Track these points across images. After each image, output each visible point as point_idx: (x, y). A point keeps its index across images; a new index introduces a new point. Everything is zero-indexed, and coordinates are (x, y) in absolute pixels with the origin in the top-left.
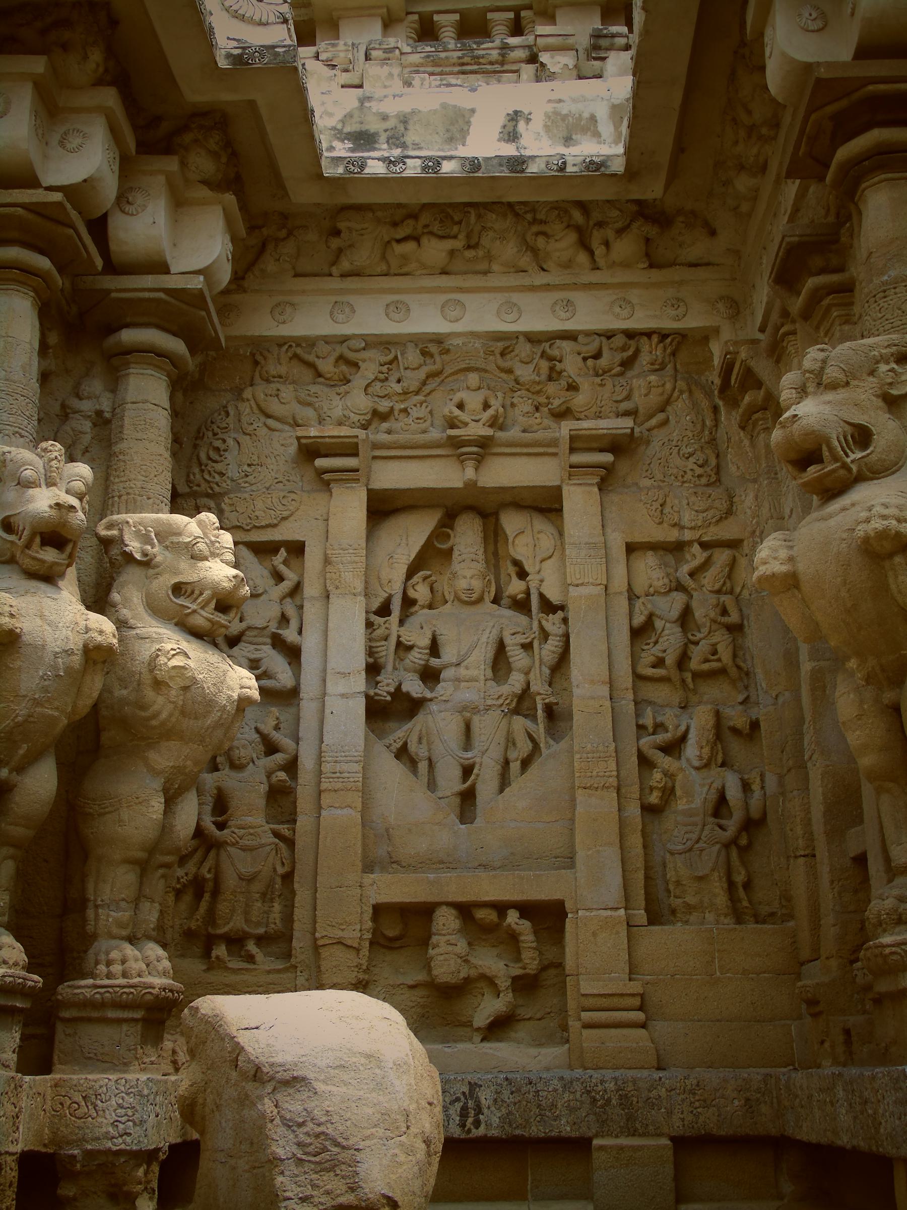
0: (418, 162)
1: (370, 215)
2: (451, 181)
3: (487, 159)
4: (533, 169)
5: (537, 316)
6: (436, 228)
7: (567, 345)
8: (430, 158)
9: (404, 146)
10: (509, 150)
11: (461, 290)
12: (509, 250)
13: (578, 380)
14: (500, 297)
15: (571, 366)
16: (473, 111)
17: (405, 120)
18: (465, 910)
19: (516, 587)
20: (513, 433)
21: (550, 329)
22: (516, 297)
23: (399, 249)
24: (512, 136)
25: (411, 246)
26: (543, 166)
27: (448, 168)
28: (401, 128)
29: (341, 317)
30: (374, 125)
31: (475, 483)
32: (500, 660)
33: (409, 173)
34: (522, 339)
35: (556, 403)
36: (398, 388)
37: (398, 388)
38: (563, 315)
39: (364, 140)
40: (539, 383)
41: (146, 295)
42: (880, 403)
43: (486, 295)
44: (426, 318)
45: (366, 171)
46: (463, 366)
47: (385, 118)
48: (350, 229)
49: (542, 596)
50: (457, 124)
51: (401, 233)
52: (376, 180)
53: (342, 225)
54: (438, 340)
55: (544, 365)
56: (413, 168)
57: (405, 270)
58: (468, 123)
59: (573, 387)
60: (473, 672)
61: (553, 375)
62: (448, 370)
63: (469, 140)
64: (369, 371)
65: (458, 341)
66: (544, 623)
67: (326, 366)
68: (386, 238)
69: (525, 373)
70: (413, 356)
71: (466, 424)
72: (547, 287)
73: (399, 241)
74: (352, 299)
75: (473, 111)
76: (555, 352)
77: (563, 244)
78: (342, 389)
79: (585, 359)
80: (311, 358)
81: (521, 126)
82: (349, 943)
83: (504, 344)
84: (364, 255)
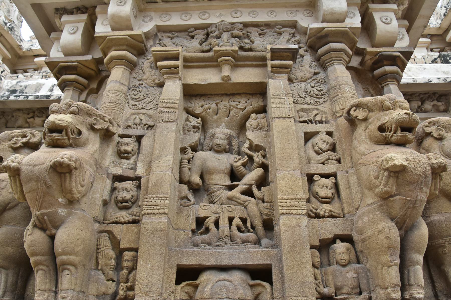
0: (23, 97)
1: (22, 111)
3: (41, 96)
6: (38, 115)
8: (26, 96)
9: (23, 93)
10: (49, 93)
16: (44, 84)
17: (26, 87)
25: (32, 120)
28: (24, 88)
30: (18, 88)
33: (20, 99)
39: (13, 92)
42: (10, 149)
45: (9, 99)
47: (21, 86)
48: (16, 115)
50: (39, 87)
51: (29, 116)
52: (11, 101)
53: (14, 114)
56: (21, 98)
58: (41, 87)
63: (40, 91)
73: (29, 118)
75: (44, 84)
84: (20, 122)
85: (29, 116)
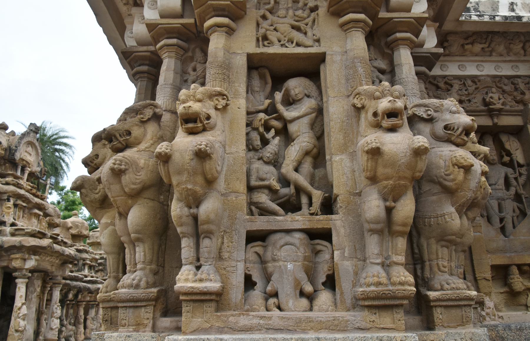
0: (488, 17)
2: (498, 23)
4: (524, 20)
5: (506, 70)
7: (519, 80)
11: (482, 61)
12: (501, 48)
13: (524, 91)
14: (494, 64)
15: (522, 86)
18: (519, 267)
19: (506, 159)
20: (508, 107)
21: (513, 74)
22: (499, 64)
23: (466, 47)
24: (513, 10)
26: (527, 19)
27: (497, 19)
28: (477, 6)
29: (444, 69)
31: (497, 123)
32: (507, 184)
33: (486, 20)
34: (503, 77)
35: (518, 98)
36: (466, 93)
37: (466, 93)
38: (516, 70)
40: (511, 92)
41: (425, 54)
43: (490, 63)
44: (471, 70)
46: (486, 86)
49: (517, 162)
51: (468, 42)
52: (475, 22)
54: (476, 76)
55: (513, 86)
57: (464, 54)
58: (498, 5)
59: (523, 93)
60: (501, 187)
61: (516, 89)
62: (481, 87)
64: (456, 87)
65: (483, 78)
66: (520, 171)
67: (442, 85)
68: (462, 43)
69: (507, 88)
70: (469, 82)
71: (495, 104)
72: (510, 61)
74: (447, 63)
76: (516, 82)
77: (517, 47)
78: (449, 92)
79: (525, 84)
80: (436, 82)
81: (515, 7)
82: (488, 278)
83: (497, 79)
85: (468, 42)
